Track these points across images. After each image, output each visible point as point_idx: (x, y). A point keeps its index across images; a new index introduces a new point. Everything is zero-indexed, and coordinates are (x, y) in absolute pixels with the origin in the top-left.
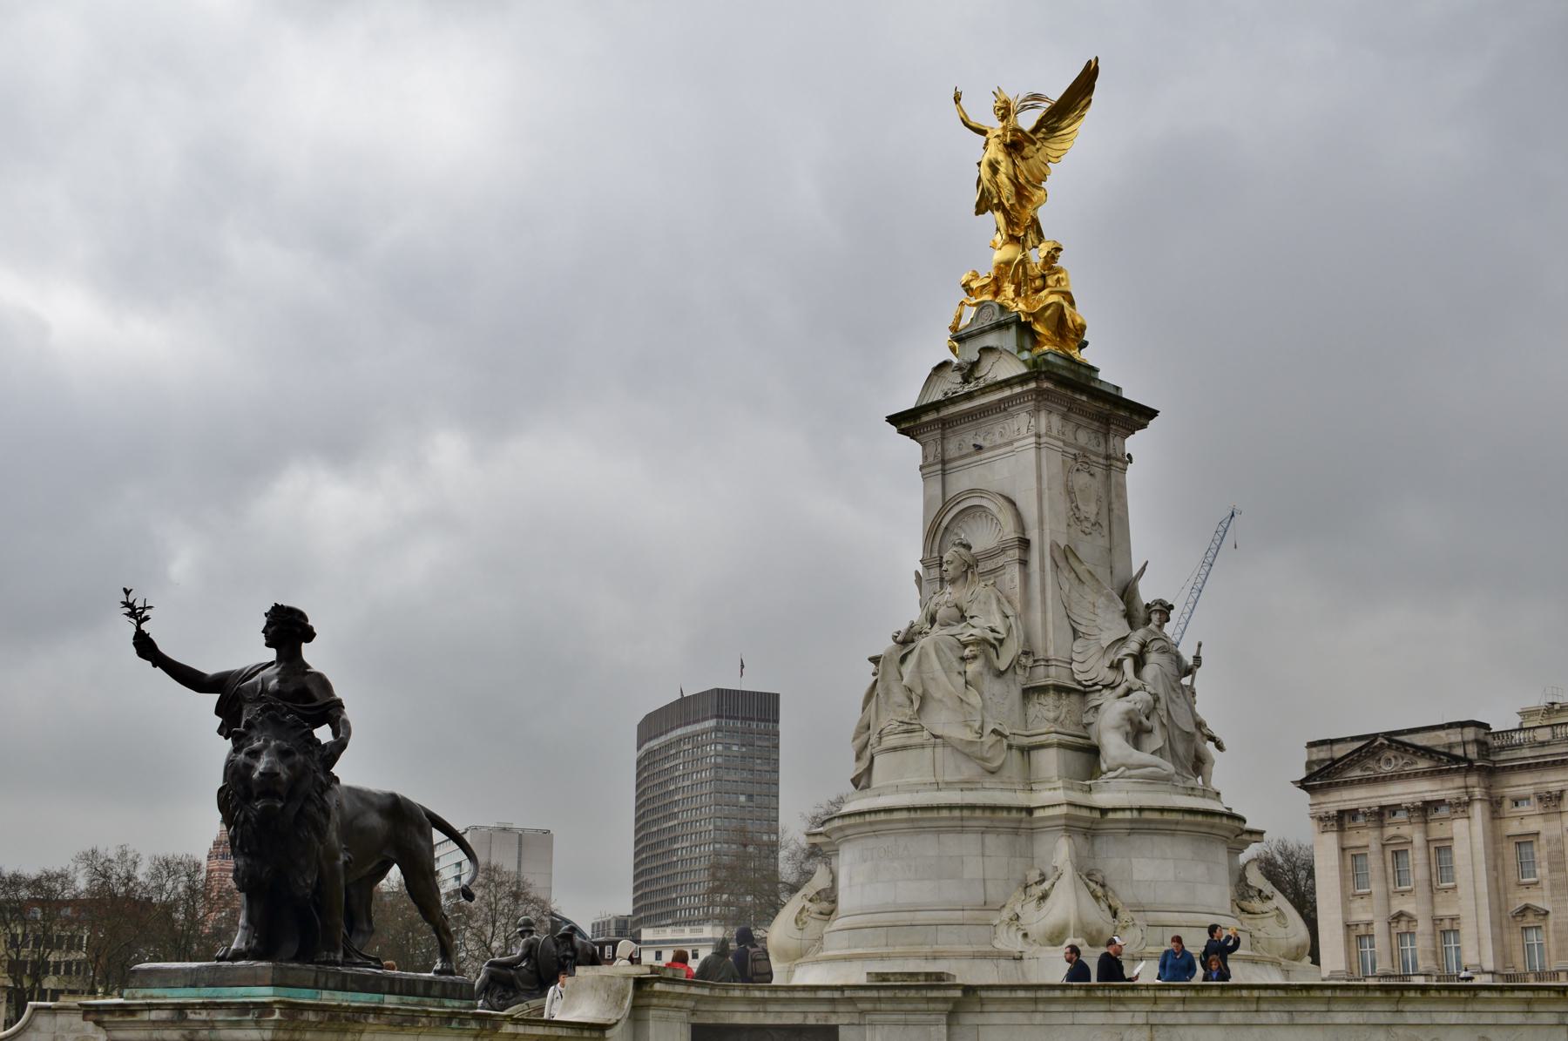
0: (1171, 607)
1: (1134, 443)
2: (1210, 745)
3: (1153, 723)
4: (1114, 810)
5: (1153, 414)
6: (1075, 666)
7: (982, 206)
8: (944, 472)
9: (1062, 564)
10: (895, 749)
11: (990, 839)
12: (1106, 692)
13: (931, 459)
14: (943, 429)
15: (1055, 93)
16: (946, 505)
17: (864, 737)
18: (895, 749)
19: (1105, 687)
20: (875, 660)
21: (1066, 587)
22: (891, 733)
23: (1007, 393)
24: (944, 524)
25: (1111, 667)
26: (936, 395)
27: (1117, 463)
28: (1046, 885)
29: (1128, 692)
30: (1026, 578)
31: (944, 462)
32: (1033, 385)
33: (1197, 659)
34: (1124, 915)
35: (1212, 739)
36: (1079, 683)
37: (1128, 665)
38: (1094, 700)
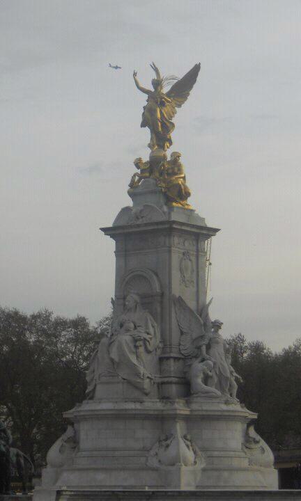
5: (217, 230)
28: (168, 442)
29: (203, 360)
30: (162, 308)
34: (199, 453)
36: (183, 355)
37: (204, 348)
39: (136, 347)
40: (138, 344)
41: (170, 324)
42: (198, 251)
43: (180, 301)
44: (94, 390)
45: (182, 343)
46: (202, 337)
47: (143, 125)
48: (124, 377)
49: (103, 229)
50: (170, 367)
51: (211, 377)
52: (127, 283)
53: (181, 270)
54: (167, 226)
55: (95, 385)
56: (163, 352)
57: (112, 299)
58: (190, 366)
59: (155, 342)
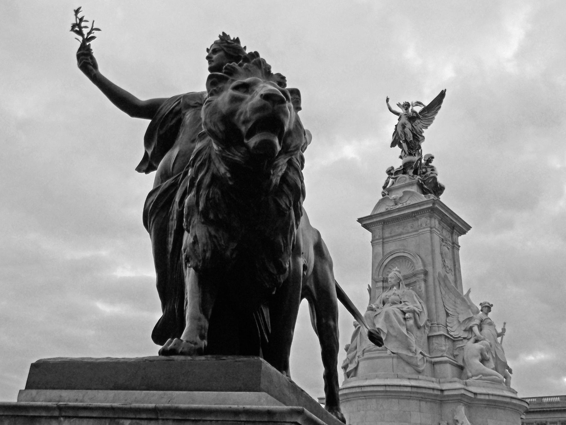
0: (492, 305)
1: (461, 239)
3: (488, 356)
4: (481, 394)
6: (448, 328)
8: (383, 243)
9: (442, 283)
11: (423, 404)
12: (465, 341)
15: (427, 103)
16: (385, 257)
21: (444, 293)
24: (385, 264)
25: (465, 330)
26: (382, 210)
27: (455, 246)
29: (476, 341)
30: (427, 287)
31: (383, 239)
33: (504, 330)
36: (451, 336)
37: (476, 329)
42: (453, 243)
44: (356, 369)
45: (448, 324)
46: (470, 319)
47: (393, 145)
49: (360, 220)
52: (386, 266)
53: (441, 254)
54: (431, 205)
55: (358, 363)
57: (369, 285)
58: (462, 348)
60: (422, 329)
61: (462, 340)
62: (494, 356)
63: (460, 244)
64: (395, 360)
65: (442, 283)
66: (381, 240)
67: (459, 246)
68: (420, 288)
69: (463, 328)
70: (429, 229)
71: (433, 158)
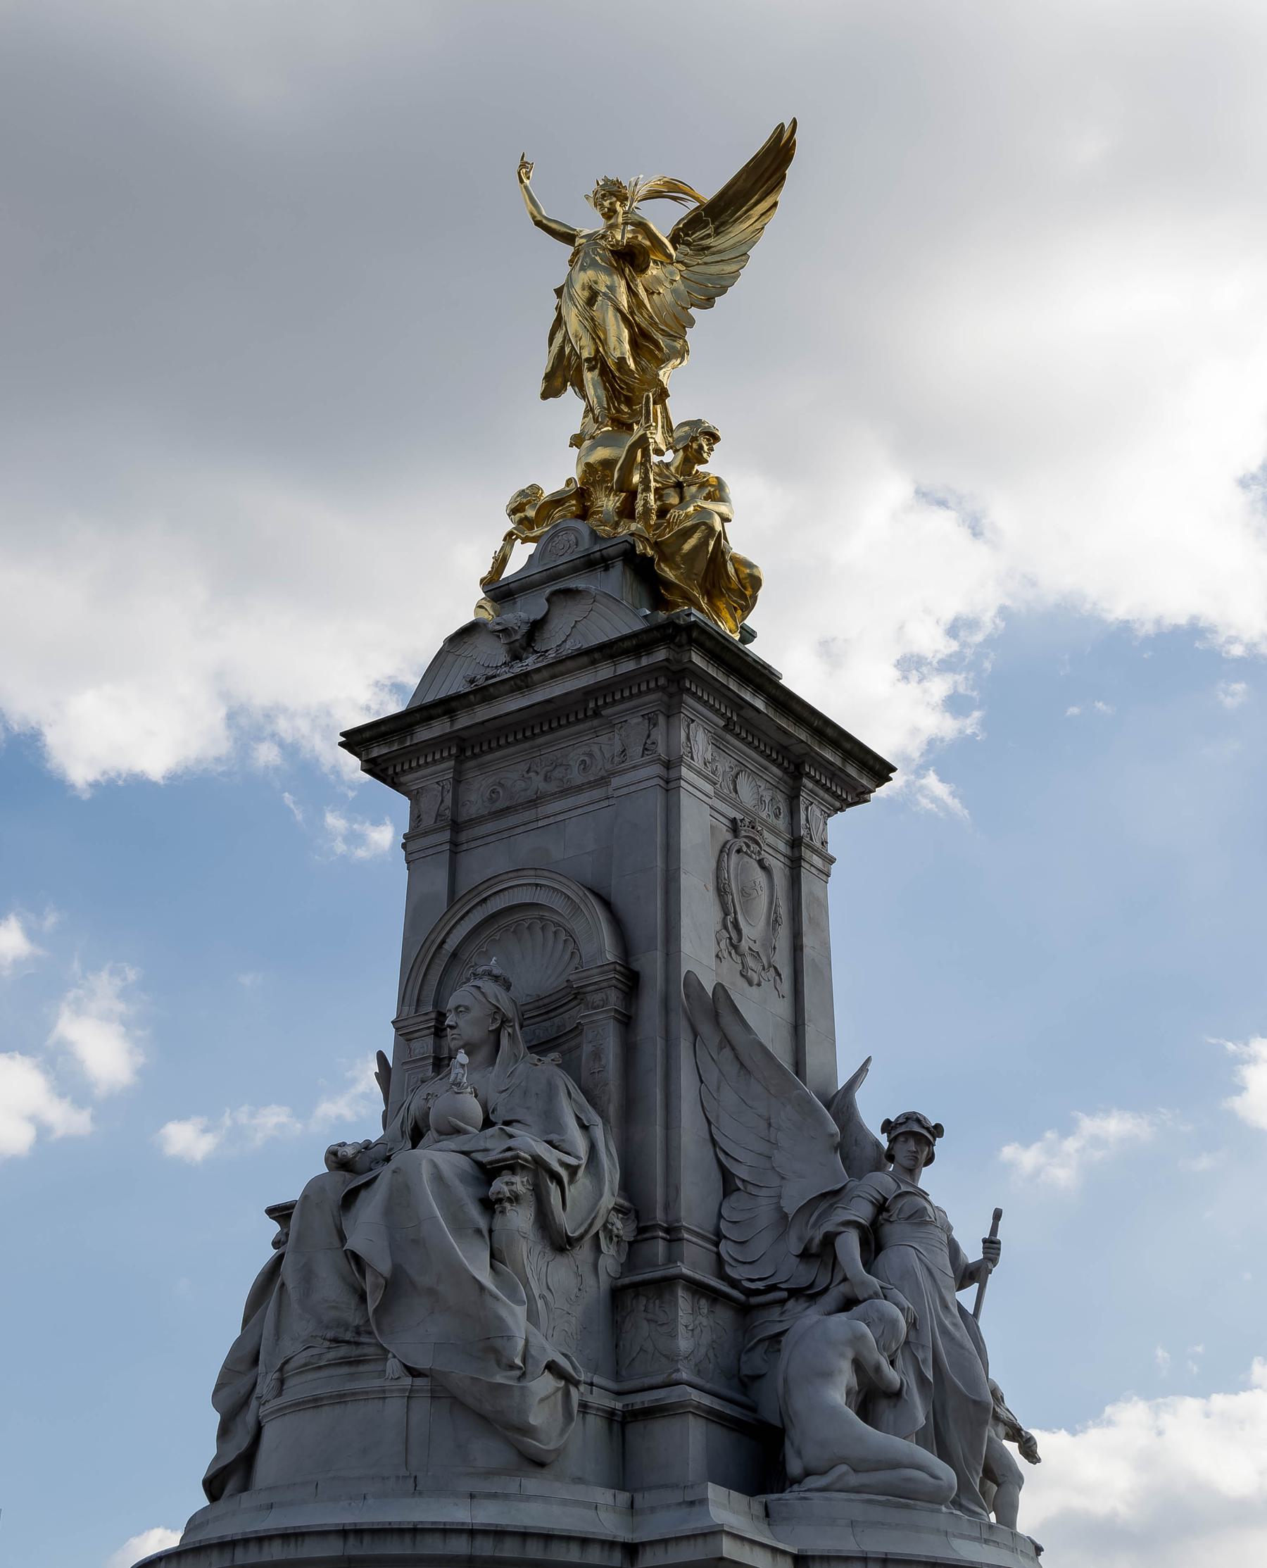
1: (843, 831)
2: (1012, 1447)
6: (724, 1247)
7: (561, 376)
8: (455, 846)
9: (705, 1028)
10: (315, 1403)
13: (428, 821)
14: (460, 758)
15: (708, 190)
17: (243, 1384)
18: (315, 1403)
19: (795, 1293)
20: (280, 1213)
21: (712, 1077)
22: (306, 1368)
23: (605, 672)
26: (454, 685)
29: (848, 1304)
30: (629, 1051)
31: (456, 826)
32: (661, 655)
33: (991, 1246)
35: (1015, 1433)
36: (734, 1283)
37: (850, 1245)
38: (771, 1323)
39: (490, 1206)
40: (500, 1186)
41: (670, 1123)
42: (796, 843)
43: (717, 1010)
48: (422, 1363)
50: (673, 1335)
51: (896, 1395)
52: (454, 955)
53: (722, 891)
56: (633, 1251)
57: (381, 1057)
59: (588, 1200)
60: (583, 1253)
61: (783, 1302)
62: (930, 1375)
63: (831, 850)
64: (422, 1407)
65: (705, 1028)
66: (446, 835)
67: (831, 860)
68: (597, 1055)
69: (796, 1248)
70: (657, 769)
71: (713, 437)
